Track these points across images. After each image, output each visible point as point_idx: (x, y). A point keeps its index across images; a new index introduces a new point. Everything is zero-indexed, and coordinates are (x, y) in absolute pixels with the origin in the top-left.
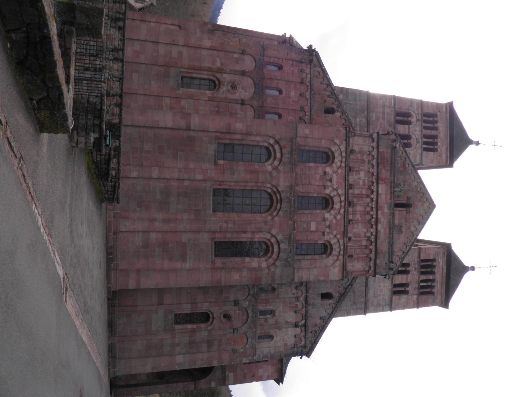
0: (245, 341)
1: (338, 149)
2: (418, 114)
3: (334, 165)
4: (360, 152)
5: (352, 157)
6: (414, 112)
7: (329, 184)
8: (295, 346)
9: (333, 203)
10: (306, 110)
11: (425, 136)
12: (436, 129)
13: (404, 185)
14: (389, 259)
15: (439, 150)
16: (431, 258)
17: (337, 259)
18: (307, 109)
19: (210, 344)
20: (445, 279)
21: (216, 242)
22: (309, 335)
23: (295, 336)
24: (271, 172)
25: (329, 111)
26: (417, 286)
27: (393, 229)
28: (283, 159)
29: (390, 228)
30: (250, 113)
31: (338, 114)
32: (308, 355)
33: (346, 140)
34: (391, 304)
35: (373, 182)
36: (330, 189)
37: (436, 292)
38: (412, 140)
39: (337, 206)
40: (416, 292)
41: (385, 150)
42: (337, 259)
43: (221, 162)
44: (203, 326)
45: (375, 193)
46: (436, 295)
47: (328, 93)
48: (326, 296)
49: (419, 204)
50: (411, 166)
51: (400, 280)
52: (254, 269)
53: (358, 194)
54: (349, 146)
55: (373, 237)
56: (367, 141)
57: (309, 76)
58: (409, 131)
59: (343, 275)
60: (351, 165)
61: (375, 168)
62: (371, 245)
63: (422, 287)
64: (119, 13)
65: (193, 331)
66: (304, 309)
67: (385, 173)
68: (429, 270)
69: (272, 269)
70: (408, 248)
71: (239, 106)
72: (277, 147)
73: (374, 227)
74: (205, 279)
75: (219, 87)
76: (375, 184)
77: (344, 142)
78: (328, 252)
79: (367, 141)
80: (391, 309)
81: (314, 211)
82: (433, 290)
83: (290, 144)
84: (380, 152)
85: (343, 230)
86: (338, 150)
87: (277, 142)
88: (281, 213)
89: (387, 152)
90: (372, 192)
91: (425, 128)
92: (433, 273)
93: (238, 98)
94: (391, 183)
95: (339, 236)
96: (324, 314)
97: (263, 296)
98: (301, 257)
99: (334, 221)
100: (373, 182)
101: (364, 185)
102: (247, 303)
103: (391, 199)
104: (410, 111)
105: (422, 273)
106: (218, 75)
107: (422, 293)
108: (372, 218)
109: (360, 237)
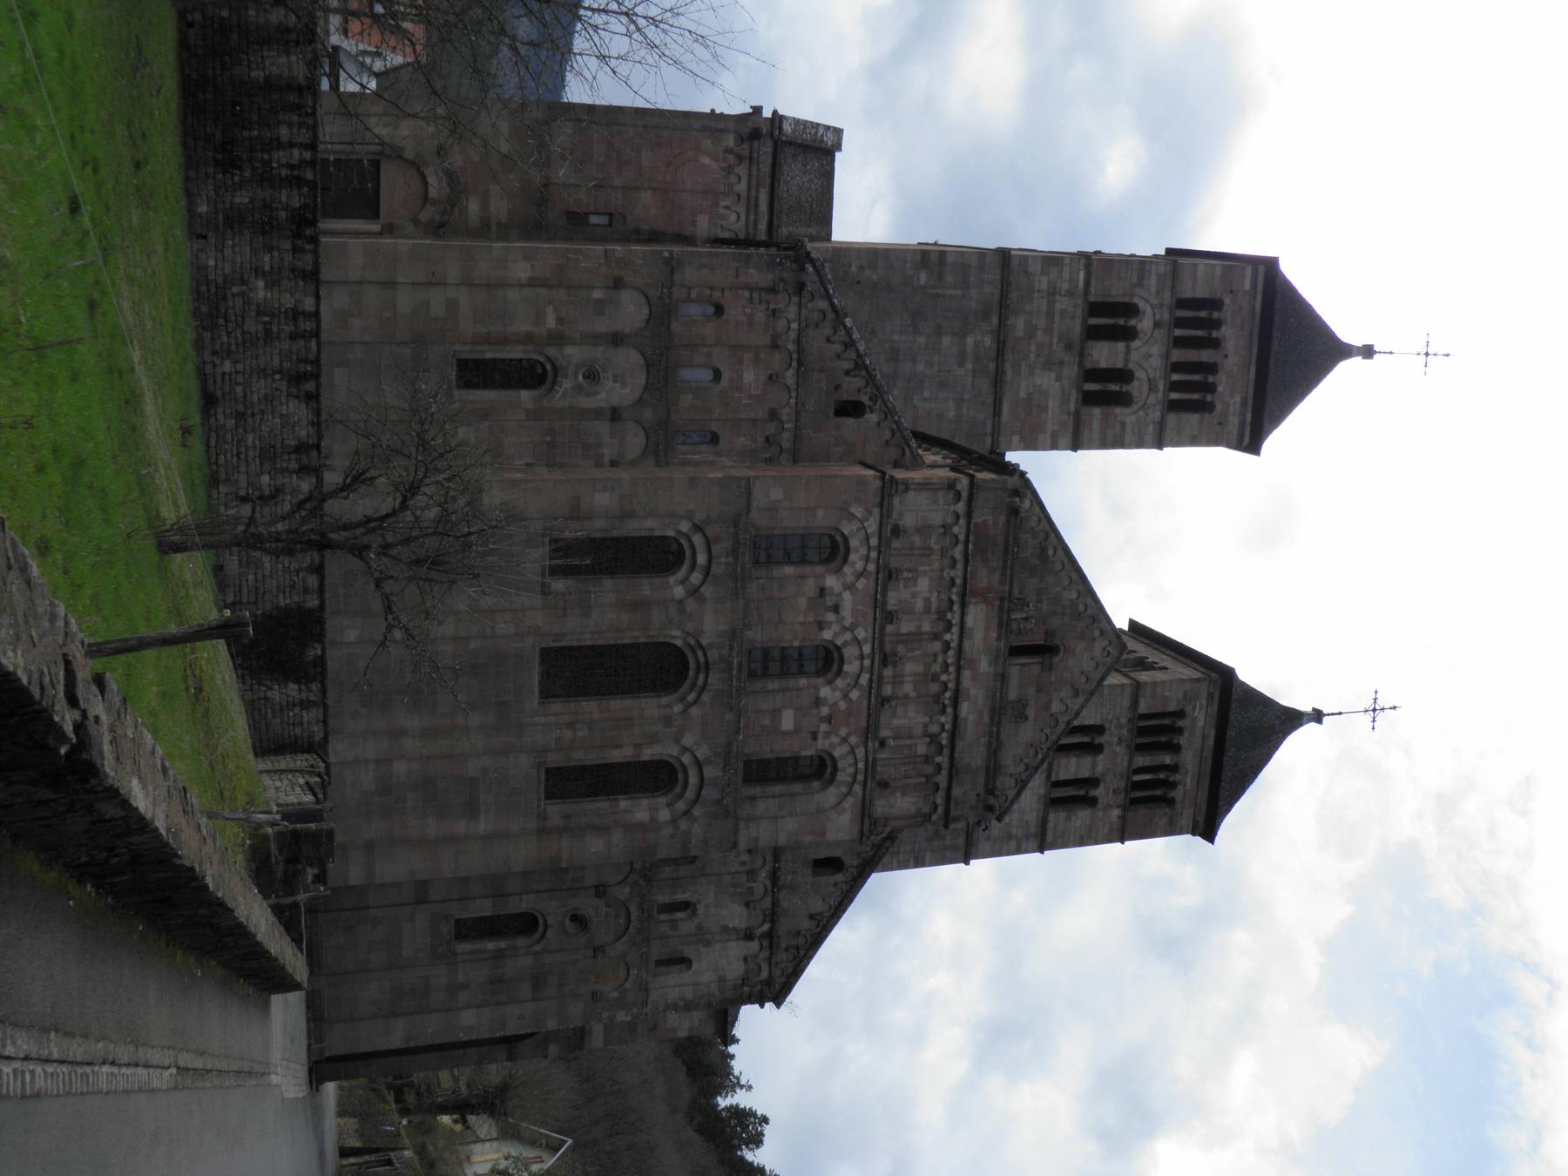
0: (623, 973)
1: (858, 530)
2: (1161, 305)
3: (847, 569)
4: (918, 530)
5: (896, 544)
6: (1147, 301)
7: (831, 617)
8: (745, 980)
9: (842, 661)
10: (784, 418)
11: (1177, 367)
12: (1215, 344)
13: (1039, 601)
14: (986, 785)
15: (1219, 407)
16: (1172, 707)
17: (849, 793)
18: (786, 413)
19: (538, 982)
20: (1209, 763)
21: (548, 771)
22: (781, 956)
23: (745, 959)
24: (681, 602)
25: (850, 409)
26: (1122, 784)
27: (1002, 711)
28: (714, 568)
29: (993, 710)
30: (635, 442)
31: (872, 418)
32: (779, 1000)
33: (881, 506)
35: (952, 603)
36: (835, 628)
38: (1136, 383)
39: (851, 668)
40: (1120, 799)
41: (990, 519)
42: (849, 793)
43: (559, 585)
44: (521, 942)
45: (955, 630)
46: (1178, 806)
47: (848, 365)
48: (829, 865)
49: (1079, 646)
50: (1060, 552)
51: (1073, 770)
52: (641, 827)
53: (910, 634)
54: (889, 516)
55: (944, 735)
56: (941, 501)
57: (794, 326)
58: (1127, 360)
59: (862, 831)
60: (894, 563)
61: (959, 566)
62: (940, 753)
64: (306, 361)
65: (499, 955)
66: (769, 899)
67: (985, 577)
68: (1163, 739)
69: (684, 824)
70: (1040, 756)
71: (603, 427)
72: (698, 540)
73: (949, 710)
74: (522, 854)
75: (554, 382)
76: (956, 607)
77: (876, 511)
78: (827, 775)
79: (941, 501)
80: (1041, 849)
81: (792, 683)
82: (1172, 794)
83: (732, 530)
84: (976, 525)
85: (864, 724)
86: (860, 528)
87: (697, 528)
88: (706, 697)
89: (996, 524)
90: (949, 626)
91: (1179, 343)
92: (1176, 749)
93: (602, 404)
94: (1002, 599)
95: (853, 740)
96: (818, 906)
97: (667, 871)
98: (756, 790)
99: (843, 705)
100: (952, 603)
101: (927, 611)
102: (627, 890)
103: (999, 639)
104: (1136, 300)
105: (1141, 748)
106: (552, 352)
107: (1135, 802)
108: (946, 689)
109: (910, 737)
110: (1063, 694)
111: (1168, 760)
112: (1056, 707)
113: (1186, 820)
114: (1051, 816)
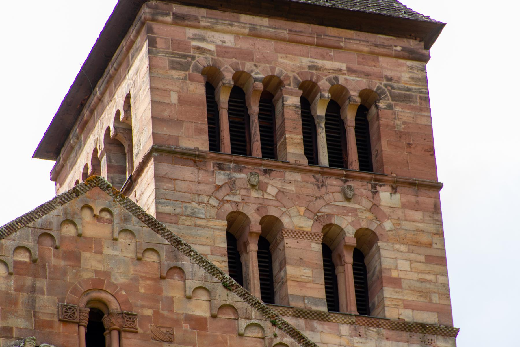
16: (198, 90)
26: (334, 184)
34: (423, 328)
37: (363, 83)
40: (361, 188)
46: (376, 84)
49: (91, 263)
51: (307, 272)
63: (338, 159)
110: (177, 295)
111: (292, 101)
112: (200, 309)
113: (402, 72)
114: (391, 313)
